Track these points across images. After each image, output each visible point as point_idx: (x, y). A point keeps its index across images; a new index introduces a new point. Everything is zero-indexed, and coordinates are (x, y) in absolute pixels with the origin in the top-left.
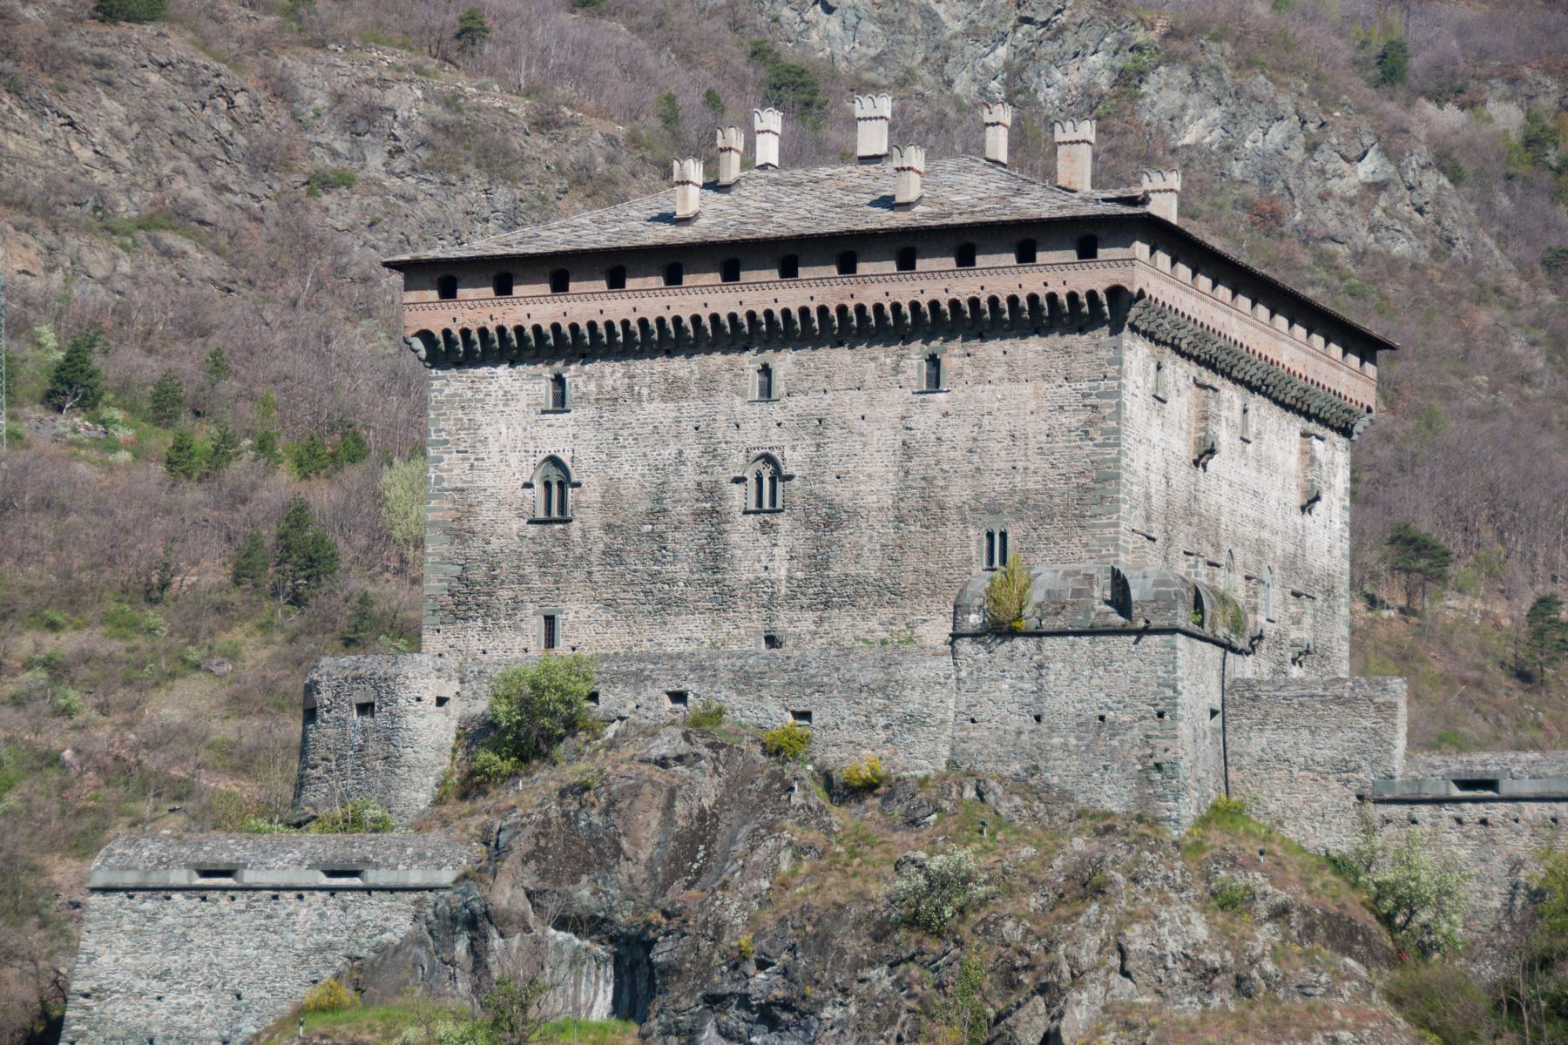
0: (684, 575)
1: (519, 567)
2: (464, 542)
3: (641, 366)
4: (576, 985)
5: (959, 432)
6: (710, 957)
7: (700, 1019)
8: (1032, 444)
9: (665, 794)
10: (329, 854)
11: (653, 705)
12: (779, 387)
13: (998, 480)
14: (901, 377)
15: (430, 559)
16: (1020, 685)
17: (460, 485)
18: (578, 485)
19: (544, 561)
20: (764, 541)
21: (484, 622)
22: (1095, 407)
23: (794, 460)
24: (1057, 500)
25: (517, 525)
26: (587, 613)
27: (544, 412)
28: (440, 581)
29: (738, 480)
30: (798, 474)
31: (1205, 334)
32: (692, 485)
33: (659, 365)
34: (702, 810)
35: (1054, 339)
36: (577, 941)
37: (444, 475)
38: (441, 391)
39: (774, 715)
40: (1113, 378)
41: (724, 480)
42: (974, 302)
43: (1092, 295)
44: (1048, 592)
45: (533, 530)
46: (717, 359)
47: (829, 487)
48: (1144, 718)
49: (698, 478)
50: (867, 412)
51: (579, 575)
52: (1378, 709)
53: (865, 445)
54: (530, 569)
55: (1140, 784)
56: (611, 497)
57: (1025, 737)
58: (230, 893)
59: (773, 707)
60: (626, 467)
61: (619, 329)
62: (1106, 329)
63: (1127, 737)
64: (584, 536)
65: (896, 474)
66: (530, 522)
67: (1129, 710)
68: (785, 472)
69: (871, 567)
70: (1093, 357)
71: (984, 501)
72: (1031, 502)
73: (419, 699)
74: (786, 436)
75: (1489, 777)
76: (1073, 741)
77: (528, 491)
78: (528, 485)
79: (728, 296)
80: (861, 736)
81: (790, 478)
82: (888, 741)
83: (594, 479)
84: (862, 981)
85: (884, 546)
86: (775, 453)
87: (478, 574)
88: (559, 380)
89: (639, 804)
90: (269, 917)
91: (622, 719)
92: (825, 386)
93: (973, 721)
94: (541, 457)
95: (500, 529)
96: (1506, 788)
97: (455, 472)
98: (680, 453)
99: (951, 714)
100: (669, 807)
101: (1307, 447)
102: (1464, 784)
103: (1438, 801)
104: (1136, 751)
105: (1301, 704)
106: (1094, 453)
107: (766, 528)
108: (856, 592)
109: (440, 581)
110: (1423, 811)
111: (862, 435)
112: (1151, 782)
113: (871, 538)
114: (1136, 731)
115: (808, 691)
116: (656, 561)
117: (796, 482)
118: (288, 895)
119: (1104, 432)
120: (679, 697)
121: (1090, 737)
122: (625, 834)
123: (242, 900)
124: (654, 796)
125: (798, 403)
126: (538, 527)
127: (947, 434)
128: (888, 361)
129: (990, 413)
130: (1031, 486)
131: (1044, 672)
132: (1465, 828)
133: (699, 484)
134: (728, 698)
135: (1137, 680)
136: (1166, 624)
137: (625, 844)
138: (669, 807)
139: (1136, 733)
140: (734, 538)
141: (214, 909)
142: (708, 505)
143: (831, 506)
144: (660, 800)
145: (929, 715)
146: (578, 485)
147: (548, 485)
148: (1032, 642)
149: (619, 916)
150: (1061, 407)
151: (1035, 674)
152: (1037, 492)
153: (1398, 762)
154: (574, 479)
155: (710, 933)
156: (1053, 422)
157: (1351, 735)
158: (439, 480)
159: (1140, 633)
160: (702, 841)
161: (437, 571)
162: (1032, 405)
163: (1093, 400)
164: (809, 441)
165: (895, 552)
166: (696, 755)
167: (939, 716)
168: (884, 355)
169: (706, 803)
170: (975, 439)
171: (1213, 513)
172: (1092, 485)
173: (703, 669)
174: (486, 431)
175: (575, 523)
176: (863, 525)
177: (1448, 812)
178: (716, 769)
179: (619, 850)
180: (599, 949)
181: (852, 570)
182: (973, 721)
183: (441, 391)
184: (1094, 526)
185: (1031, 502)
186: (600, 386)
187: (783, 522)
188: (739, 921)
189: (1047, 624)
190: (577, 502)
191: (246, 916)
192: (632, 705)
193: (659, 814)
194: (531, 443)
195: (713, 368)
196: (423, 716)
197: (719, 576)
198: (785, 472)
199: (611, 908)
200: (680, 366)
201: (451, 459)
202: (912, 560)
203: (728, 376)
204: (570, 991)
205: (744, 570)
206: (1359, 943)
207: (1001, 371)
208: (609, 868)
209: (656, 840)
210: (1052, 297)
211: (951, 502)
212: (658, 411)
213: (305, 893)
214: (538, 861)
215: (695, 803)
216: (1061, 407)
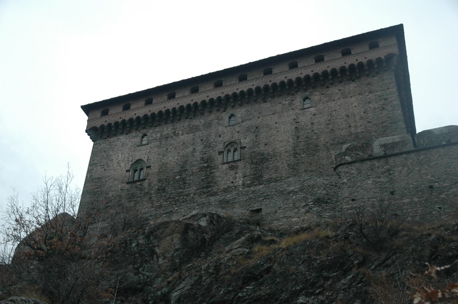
20: (232, 172)
22: (385, 99)
32: (199, 159)
49: (202, 156)
51: (146, 199)
77: (128, 173)
78: (128, 171)
117: (246, 149)
122: (158, 246)
126: (131, 184)
130: (359, 130)
140: (217, 174)
142: (206, 165)
148: (383, 161)
163: (385, 97)
175: (147, 181)
197: (210, 189)
212: (186, 138)
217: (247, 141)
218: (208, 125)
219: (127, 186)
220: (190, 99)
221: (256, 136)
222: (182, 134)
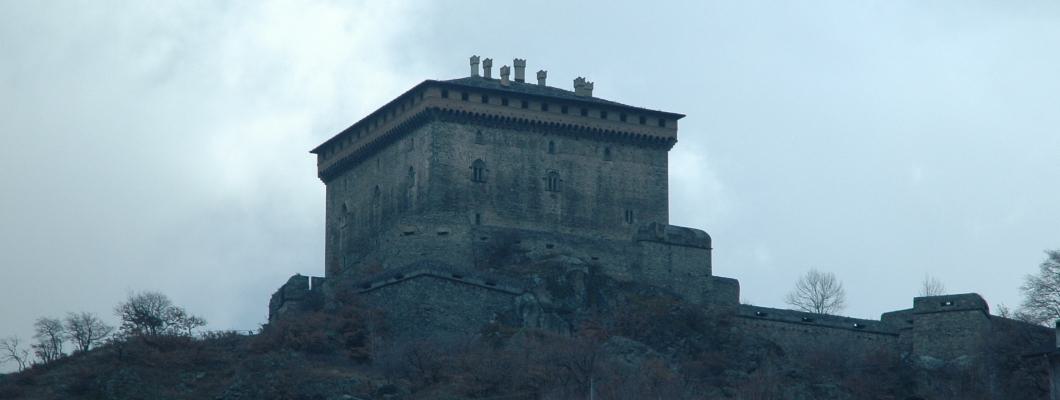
12: (557, 150)
23: (563, 174)
78: (470, 168)
140: (542, 198)
212: (518, 151)
219: (471, 183)
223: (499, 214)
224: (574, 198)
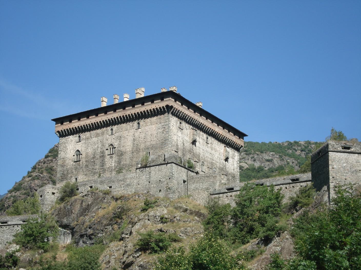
0: (98, 168)
1: (72, 170)
2: (64, 167)
3: (92, 132)
4: (64, 239)
5: (142, 135)
6: (82, 228)
7: (79, 240)
8: (154, 136)
9: (81, 201)
10: (23, 218)
11: (87, 189)
12: (114, 132)
13: (149, 143)
14: (133, 127)
15: (58, 171)
16: (146, 176)
17: (63, 157)
18: (82, 154)
19: (76, 169)
20: (111, 160)
21: (66, 181)
22: (164, 127)
23: (116, 145)
24: (158, 145)
25: (72, 163)
26: (82, 177)
27: (77, 142)
28: (60, 175)
29: (107, 149)
30: (116, 147)
31: (192, 119)
32: (100, 152)
33: (95, 132)
34: (88, 204)
35: (159, 116)
36: (65, 230)
37: (61, 156)
38: (61, 141)
39: (106, 187)
40: (168, 122)
41: (105, 150)
42: (144, 111)
43: (163, 107)
44: (152, 159)
45: (74, 163)
46: (105, 128)
47: (121, 149)
48: (167, 179)
49: (100, 150)
50: (128, 134)
51: (81, 170)
52: (214, 177)
53: (127, 140)
54: (74, 171)
55: (166, 192)
56: (87, 156)
57: (147, 186)
58: (6, 226)
59: (106, 186)
60: (89, 150)
61: (88, 125)
62: (167, 113)
63: (164, 183)
64: (82, 163)
65: (132, 144)
66: (74, 162)
67: (165, 178)
68: (114, 147)
69: (128, 162)
70: (164, 119)
71: (146, 147)
72: (154, 146)
73: (48, 193)
74: (115, 140)
75: (232, 188)
76: (155, 185)
77: (74, 157)
78: (74, 156)
79: (105, 117)
80: (119, 189)
81: (115, 148)
82: (124, 189)
83: (84, 153)
84: (106, 228)
85: (130, 158)
86: (113, 144)
87: (65, 173)
88: (79, 137)
89: (76, 203)
90: (12, 230)
91: (82, 193)
92: (121, 131)
93: (139, 184)
94: (76, 150)
95: (69, 164)
96: (235, 189)
97: (63, 155)
98: (98, 146)
99: (135, 183)
100: (82, 203)
101: (225, 149)
102: (228, 189)
103: (223, 193)
104: (166, 186)
105: (201, 178)
106: (164, 136)
107: (111, 157)
108: (125, 167)
109: (60, 175)
110: (221, 195)
111: (127, 138)
112: (168, 191)
113: (128, 156)
114: (165, 182)
115: (111, 182)
116: (93, 166)
117: (116, 148)
118: (16, 226)
119: (166, 132)
120: (91, 187)
121: (158, 184)
122: (74, 209)
123: (8, 227)
124: (79, 202)
125: (117, 135)
126: (75, 163)
127: (141, 136)
128: (131, 125)
129: (147, 131)
130: (154, 143)
131: (150, 173)
132: (228, 197)
133: (101, 151)
134: (99, 186)
135: (166, 173)
136: (171, 162)
137: (73, 211)
138: (82, 203)
139: (166, 183)
140: (106, 160)
141: (3, 229)
142: (102, 155)
143: (122, 152)
144: (80, 202)
145: (131, 184)
146: (82, 154)
147: (77, 155)
148: (149, 168)
149: (71, 224)
150: (159, 128)
151: (149, 174)
152: (155, 144)
153: (217, 188)
154: (81, 153)
155: (82, 224)
156: (158, 131)
157: (209, 183)
158: (60, 157)
159: (167, 164)
160: (88, 209)
161: (59, 173)
162: (154, 129)
163: (164, 126)
164: (118, 141)
165: (131, 159)
166: (88, 194)
167: (133, 184)
168: (131, 124)
169: (89, 203)
170: (145, 136)
171: (198, 153)
172: (164, 141)
173: (95, 181)
174: (68, 147)
175: (81, 161)
176: (127, 154)
177: (225, 195)
178: (92, 197)
179: (72, 212)
180: (68, 231)
181: (125, 163)
182: (139, 184)
183: (61, 141)
184: (164, 149)
185: (154, 146)
186: (86, 137)
187: (114, 156)
188: (88, 221)
189: (151, 165)
190: (81, 157)
191: (8, 230)
192: (84, 190)
193: (80, 205)
194: (75, 148)
195: (104, 130)
196: (49, 196)
197: (103, 167)
198: (114, 147)
199: (70, 223)
200: (99, 131)
201: (62, 153)
202: (134, 159)
203: (106, 131)
204: (63, 240)
205: (107, 165)
206: (202, 216)
207: (149, 123)
208: (70, 216)
209: (79, 210)
210: (157, 108)
211: (141, 148)
212: (95, 139)
213: (19, 225)
214: (58, 216)
215: (87, 203)
216: (159, 128)
217: (116, 144)
218: (103, 133)
220: (95, 119)
221: (120, 141)
222: (94, 137)
223: (86, 175)
224: (121, 154)
